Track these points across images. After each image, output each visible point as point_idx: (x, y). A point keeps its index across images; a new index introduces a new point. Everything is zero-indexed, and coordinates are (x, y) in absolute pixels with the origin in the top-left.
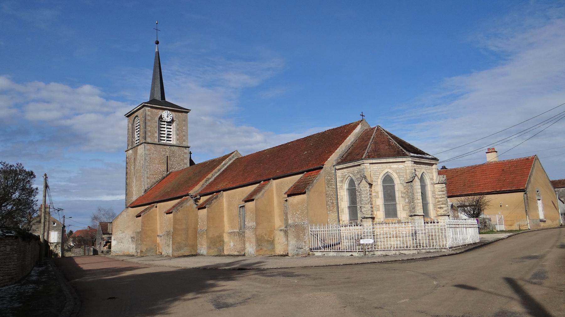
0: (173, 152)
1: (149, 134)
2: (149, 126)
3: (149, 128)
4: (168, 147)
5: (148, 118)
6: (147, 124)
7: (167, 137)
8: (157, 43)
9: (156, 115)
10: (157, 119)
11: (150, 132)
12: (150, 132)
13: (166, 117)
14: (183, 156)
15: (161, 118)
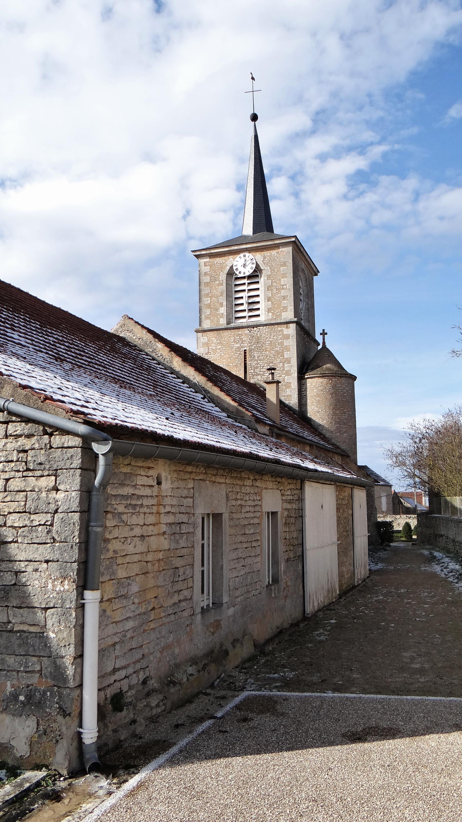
0: (258, 339)
1: (208, 312)
2: (207, 295)
3: (206, 301)
4: (246, 331)
5: (206, 279)
6: (203, 293)
7: (250, 310)
8: (254, 118)
9: (222, 268)
10: (223, 277)
11: (209, 306)
12: (209, 306)
13: (241, 269)
14: (282, 343)
15: (231, 273)
